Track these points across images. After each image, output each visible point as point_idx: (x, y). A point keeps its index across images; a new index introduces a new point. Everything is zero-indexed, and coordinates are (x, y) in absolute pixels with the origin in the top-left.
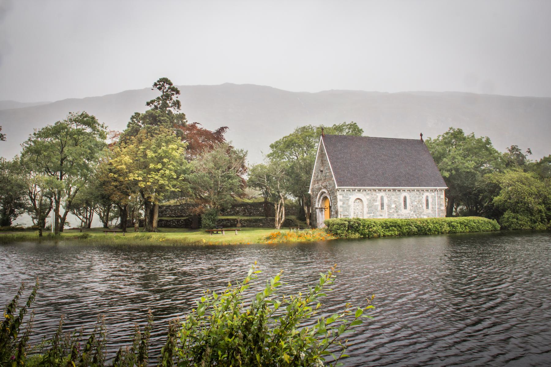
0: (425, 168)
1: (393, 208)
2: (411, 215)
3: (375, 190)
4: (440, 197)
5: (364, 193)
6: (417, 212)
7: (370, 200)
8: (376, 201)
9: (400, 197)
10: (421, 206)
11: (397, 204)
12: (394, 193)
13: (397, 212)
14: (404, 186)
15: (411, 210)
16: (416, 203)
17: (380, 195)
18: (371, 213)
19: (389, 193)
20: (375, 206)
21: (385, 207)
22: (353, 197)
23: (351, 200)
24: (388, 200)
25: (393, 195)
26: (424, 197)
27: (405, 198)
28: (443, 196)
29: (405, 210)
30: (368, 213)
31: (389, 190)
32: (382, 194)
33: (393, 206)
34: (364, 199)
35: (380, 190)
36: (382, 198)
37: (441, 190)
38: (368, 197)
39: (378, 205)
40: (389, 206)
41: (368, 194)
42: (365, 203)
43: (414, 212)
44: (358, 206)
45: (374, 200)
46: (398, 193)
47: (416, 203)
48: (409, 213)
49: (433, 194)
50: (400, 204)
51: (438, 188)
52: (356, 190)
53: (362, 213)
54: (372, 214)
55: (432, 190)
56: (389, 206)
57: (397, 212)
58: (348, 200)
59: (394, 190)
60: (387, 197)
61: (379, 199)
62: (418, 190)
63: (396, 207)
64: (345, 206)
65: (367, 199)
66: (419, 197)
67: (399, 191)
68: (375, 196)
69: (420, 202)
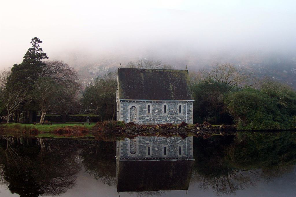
2: (168, 117)
3: (144, 102)
10: (175, 111)
11: (159, 110)
12: (157, 104)
15: (168, 114)
16: (172, 110)
17: (147, 105)
19: (154, 103)
20: (145, 110)
21: (151, 112)
22: (130, 106)
23: (128, 107)
25: (157, 104)
26: (178, 106)
27: (165, 106)
31: (154, 102)
32: (149, 104)
33: (157, 111)
35: (147, 102)
36: (149, 106)
38: (140, 106)
39: (146, 110)
41: (140, 104)
42: (138, 110)
44: (134, 110)
46: (160, 103)
47: (172, 110)
49: (185, 104)
50: (161, 110)
54: (142, 116)
55: (183, 102)
57: (159, 114)
59: (157, 102)
60: (153, 106)
61: (147, 106)
62: (174, 102)
63: (158, 111)
66: (174, 106)
67: (161, 102)
68: (144, 105)
69: (175, 109)
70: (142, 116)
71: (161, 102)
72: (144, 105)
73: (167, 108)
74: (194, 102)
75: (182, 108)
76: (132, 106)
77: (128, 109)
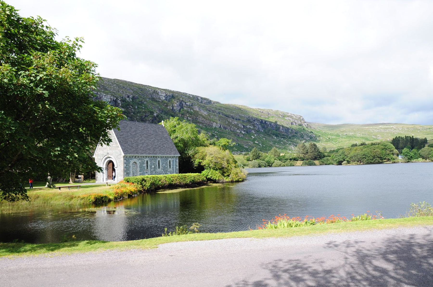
0: (167, 143)
1: (153, 168)
5: (138, 158)
6: (165, 170)
7: (141, 163)
8: (144, 163)
9: (156, 161)
11: (155, 165)
13: (155, 170)
15: (162, 169)
16: (164, 165)
17: (146, 160)
18: (142, 171)
21: (149, 167)
23: (131, 163)
24: (150, 163)
25: (153, 160)
26: (169, 161)
27: (159, 161)
28: (178, 161)
33: (153, 167)
34: (138, 163)
37: (177, 157)
38: (140, 161)
40: (151, 166)
41: (140, 159)
42: (138, 165)
43: (164, 170)
46: (156, 159)
47: (164, 165)
48: (161, 171)
49: (173, 159)
52: (134, 157)
54: (142, 172)
56: (151, 166)
60: (150, 161)
61: (146, 162)
63: (154, 167)
64: (127, 167)
65: (140, 162)
66: (166, 161)
69: (166, 163)
70: (142, 172)
72: (144, 161)
73: (160, 164)
74: (179, 157)
75: (171, 163)
76: (134, 162)
77: (130, 165)
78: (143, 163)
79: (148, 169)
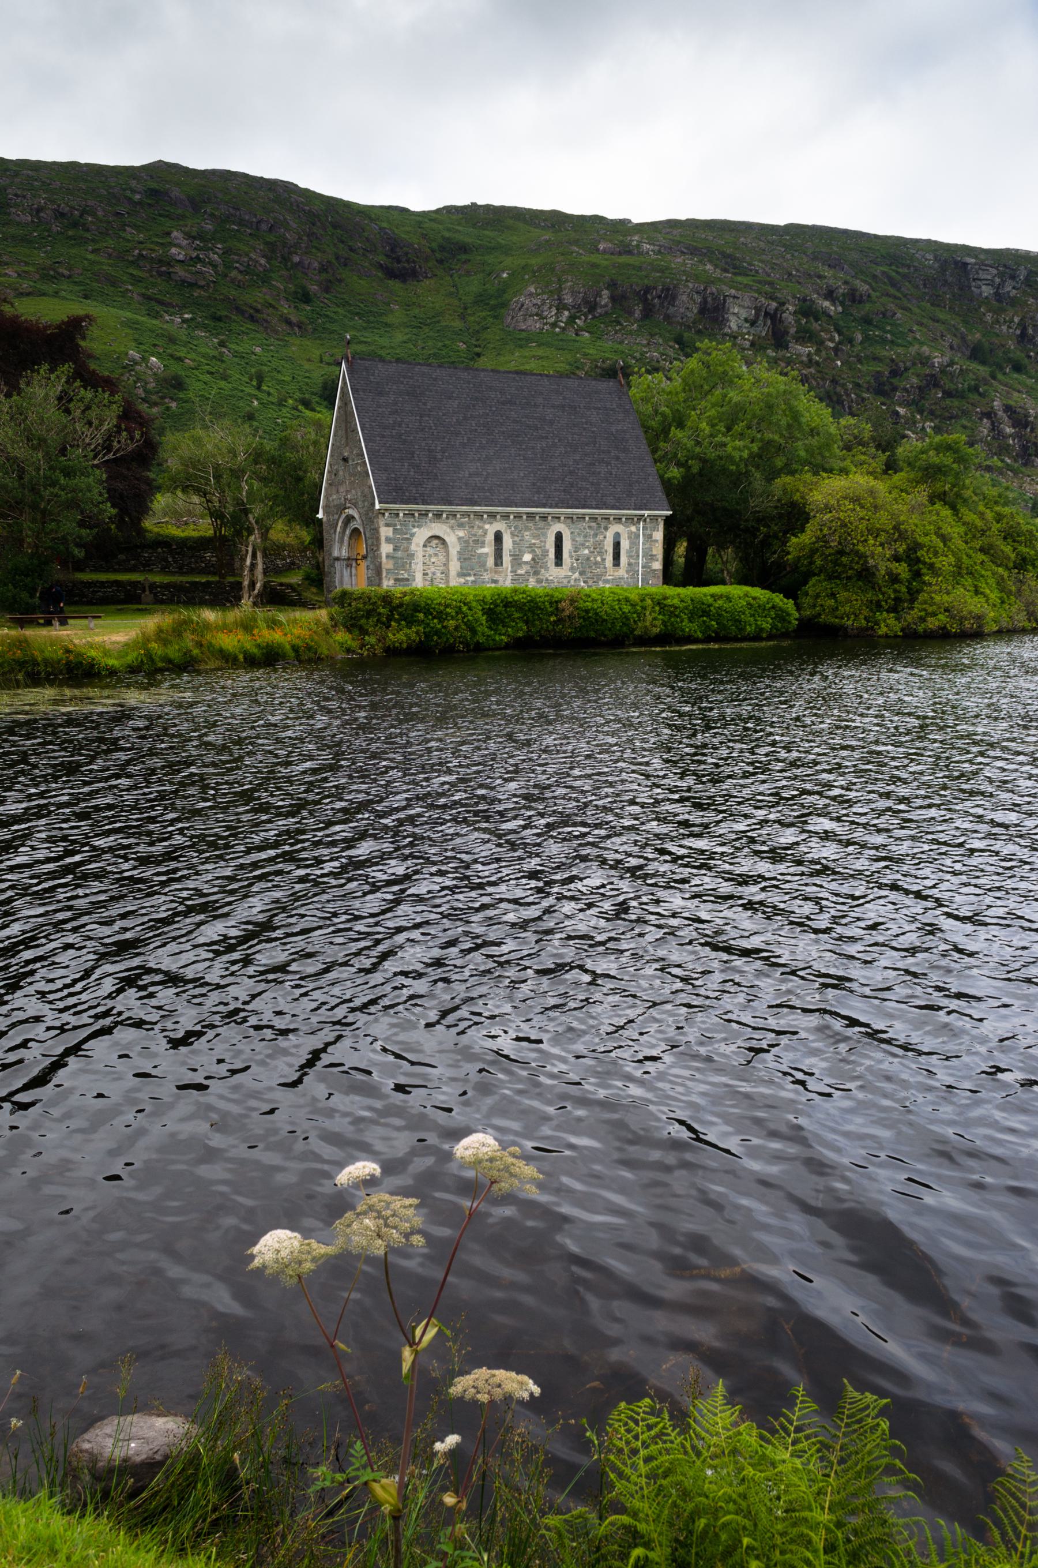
1: (526, 563)
3: (479, 516)
4: (651, 536)
5: (452, 521)
7: (467, 542)
8: (483, 543)
9: (545, 535)
10: (599, 559)
11: (538, 552)
13: (536, 573)
14: (557, 507)
16: (586, 552)
17: (491, 529)
19: (519, 523)
20: (480, 555)
22: (421, 534)
25: (527, 529)
28: (659, 535)
29: (558, 569)
30: (461, 575)
31: (518, 516)
32: (499, 525)
33: (527, 557)
34: (451, 539)
35: (492, 516)
36: (498, 537)
37: (654, 519)
38: (461, 533)
40: (516, 559)
41: (461, 526)
42: (454, 549)
43: (581, 574)
45: (476, 542)
46: (541, 524)
47: (586, 552)
49: (633, 529)
51: (646, 513)
53: (446, 573)
54: (472, 578)
55: (630, 520)
56: (516, 559)
58: (408, 539)
59: (531, 516)
61: (490, 537)
64: (399, 554)
65: (459, 539)
66: (596, 535)
69: (598, 548)
70: (472, 578)
71: (544, 518)
77: (413, 547)
78: (480, 543)
79: (500, 569)
